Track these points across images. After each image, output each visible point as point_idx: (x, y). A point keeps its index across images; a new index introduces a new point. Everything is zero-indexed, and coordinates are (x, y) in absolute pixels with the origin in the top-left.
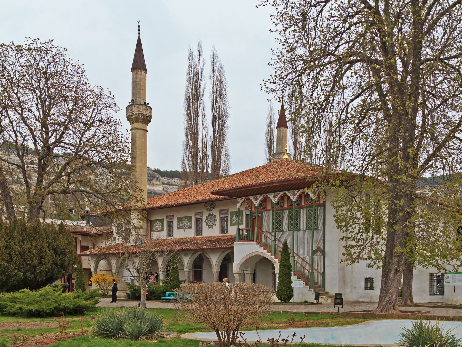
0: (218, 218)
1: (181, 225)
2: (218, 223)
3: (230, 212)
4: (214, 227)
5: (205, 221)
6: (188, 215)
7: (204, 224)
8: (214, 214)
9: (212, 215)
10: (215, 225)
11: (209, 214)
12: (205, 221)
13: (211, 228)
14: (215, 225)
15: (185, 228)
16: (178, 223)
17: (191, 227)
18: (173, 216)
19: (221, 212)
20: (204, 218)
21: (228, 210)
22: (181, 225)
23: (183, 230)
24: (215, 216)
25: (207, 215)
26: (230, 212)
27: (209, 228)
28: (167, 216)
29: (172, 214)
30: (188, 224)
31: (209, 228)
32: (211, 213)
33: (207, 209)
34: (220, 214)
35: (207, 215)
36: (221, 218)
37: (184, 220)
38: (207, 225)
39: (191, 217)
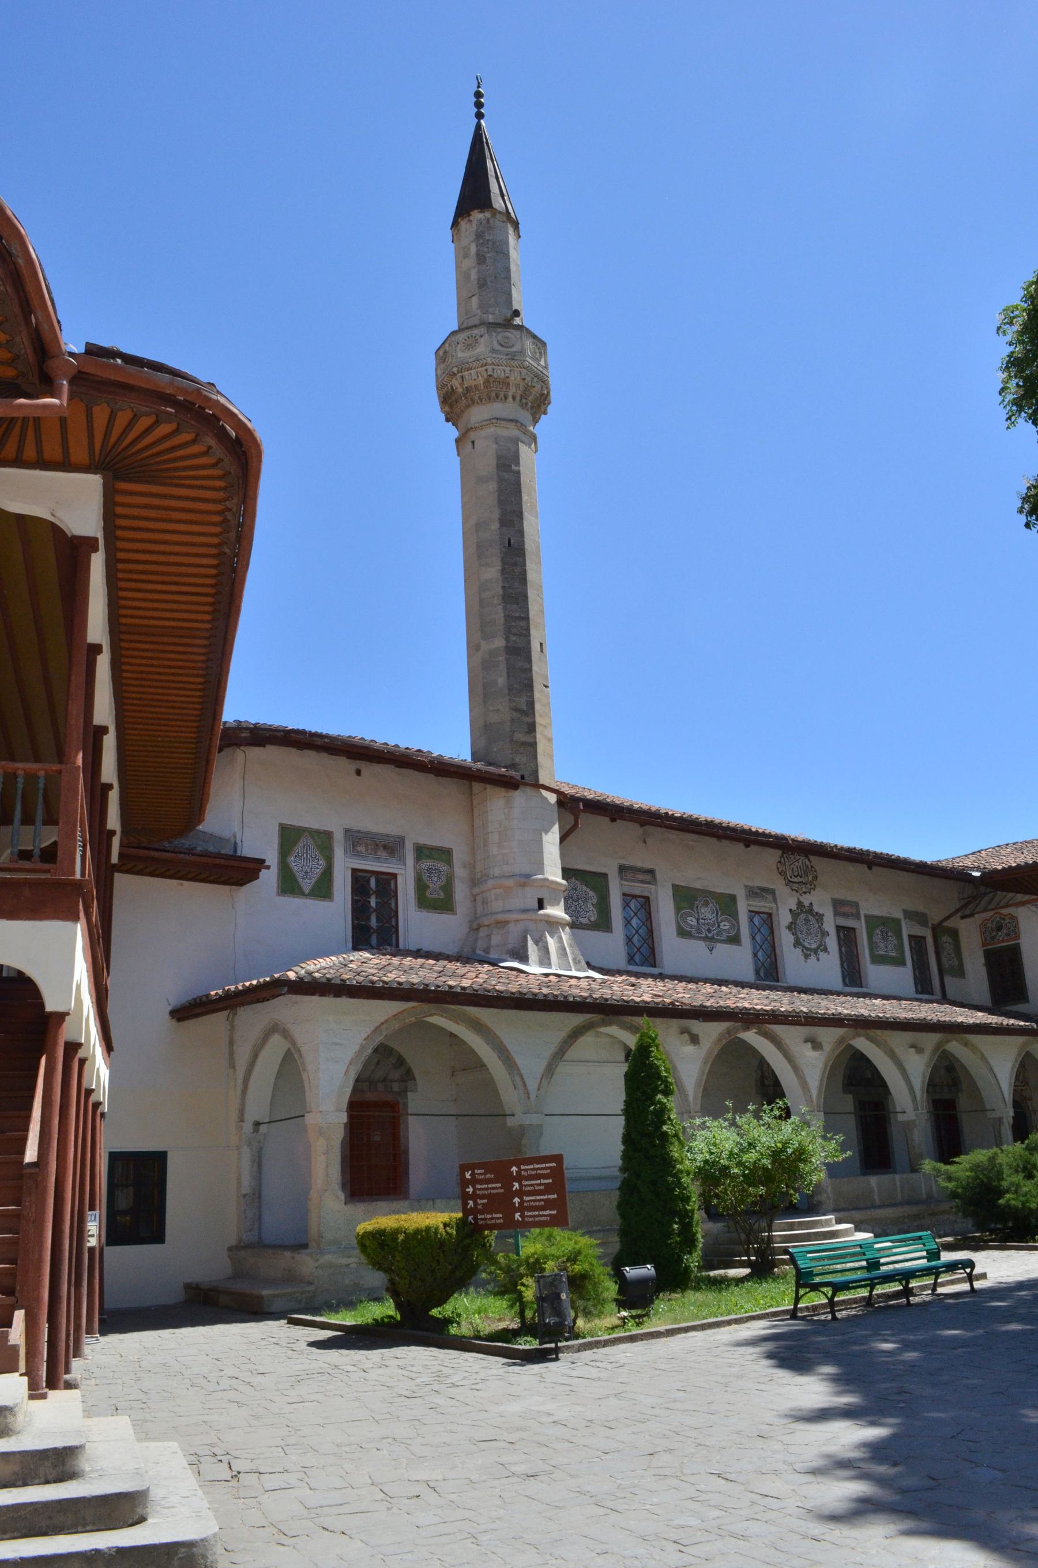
0: (829, 924)
1: (692, 921)
2: (832, 942)
3: (866, 916)
4: (822, 955)
5: (789, 928)
6: (722, 885)
7: (785, 939)
8: (816, 909)
9: (810, 911)
10: (825, 950)
11: (800, 904)
12: (789, 928)
13: (813, 958)
14: (825, 950)
15: (712, 939)
16: (678, 909)
17: (735, 940)
18: (651, 872)
19: (838, 905)
20: (784, 918)
21: (856, 905)
22: (692, 921)
23: (701, 945)
24: (819, 918)
25: (794, 907)
26: (866, 916)
27: (807, 957)
28: (622, 869)
29: (647, 865)
30: (725, 926)
31: (807, 957)
32: (806, 904)
33: (789, 883)
34: (837, 914)
35: (794, 907)
36: (839, 928)
37: (706, 904)
38: (797, 943)
39: (733, 898)
